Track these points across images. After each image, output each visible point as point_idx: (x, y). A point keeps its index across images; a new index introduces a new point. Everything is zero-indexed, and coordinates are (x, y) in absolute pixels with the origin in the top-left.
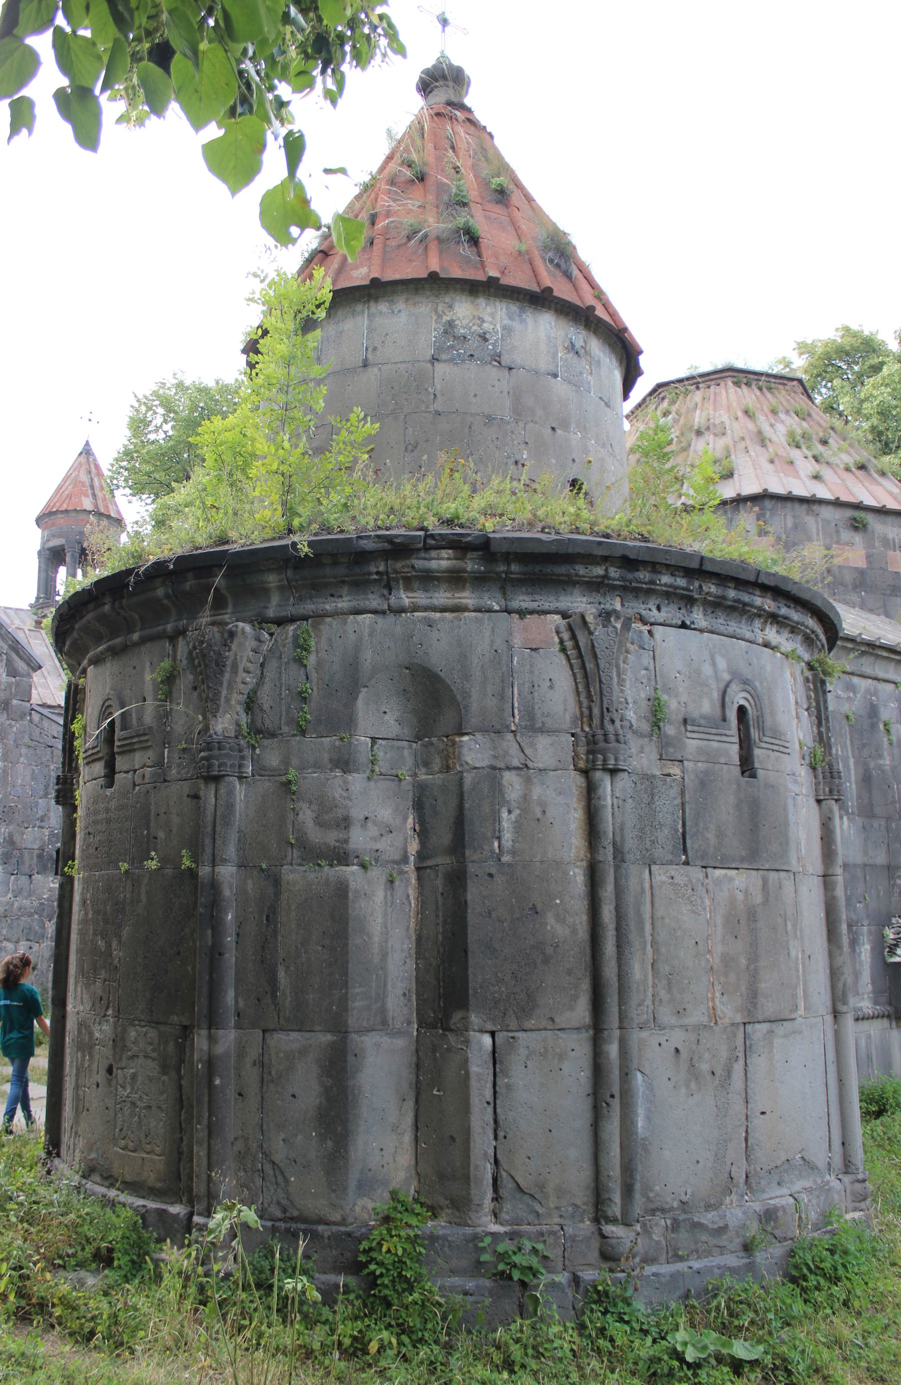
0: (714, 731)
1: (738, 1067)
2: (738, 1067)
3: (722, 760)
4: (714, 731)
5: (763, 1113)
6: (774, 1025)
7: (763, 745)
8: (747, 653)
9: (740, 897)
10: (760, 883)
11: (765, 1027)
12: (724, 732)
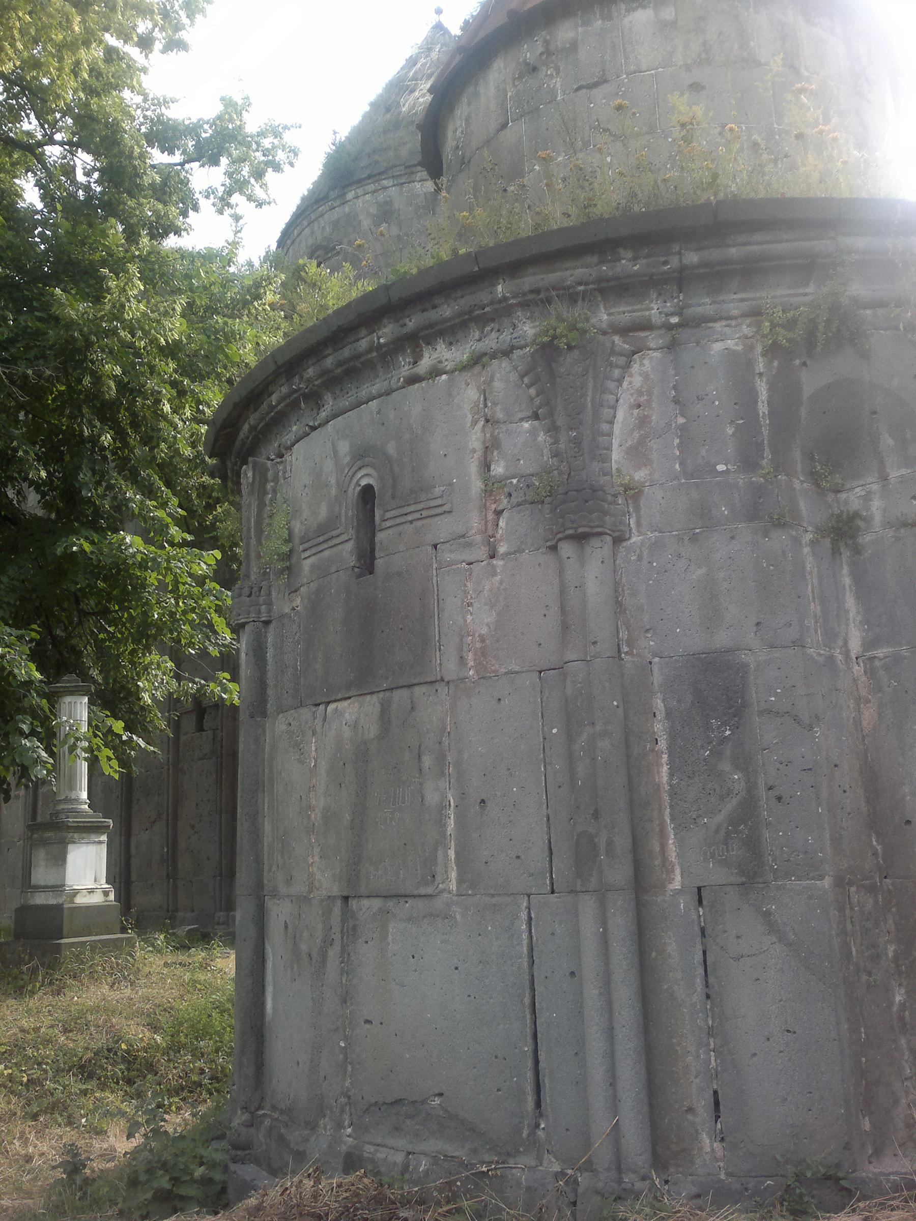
0: (321, 539)
1: (333, 953)
2: (333, 953)
3: (333, 569)
4: (321, 539)
5: (368, 1022)
6: (391, 904)
7: (388, 524)
8: (379, 412)
9: (347, 733)
10: (378, 708)
11: (377, 903)
12: (334, 533)
